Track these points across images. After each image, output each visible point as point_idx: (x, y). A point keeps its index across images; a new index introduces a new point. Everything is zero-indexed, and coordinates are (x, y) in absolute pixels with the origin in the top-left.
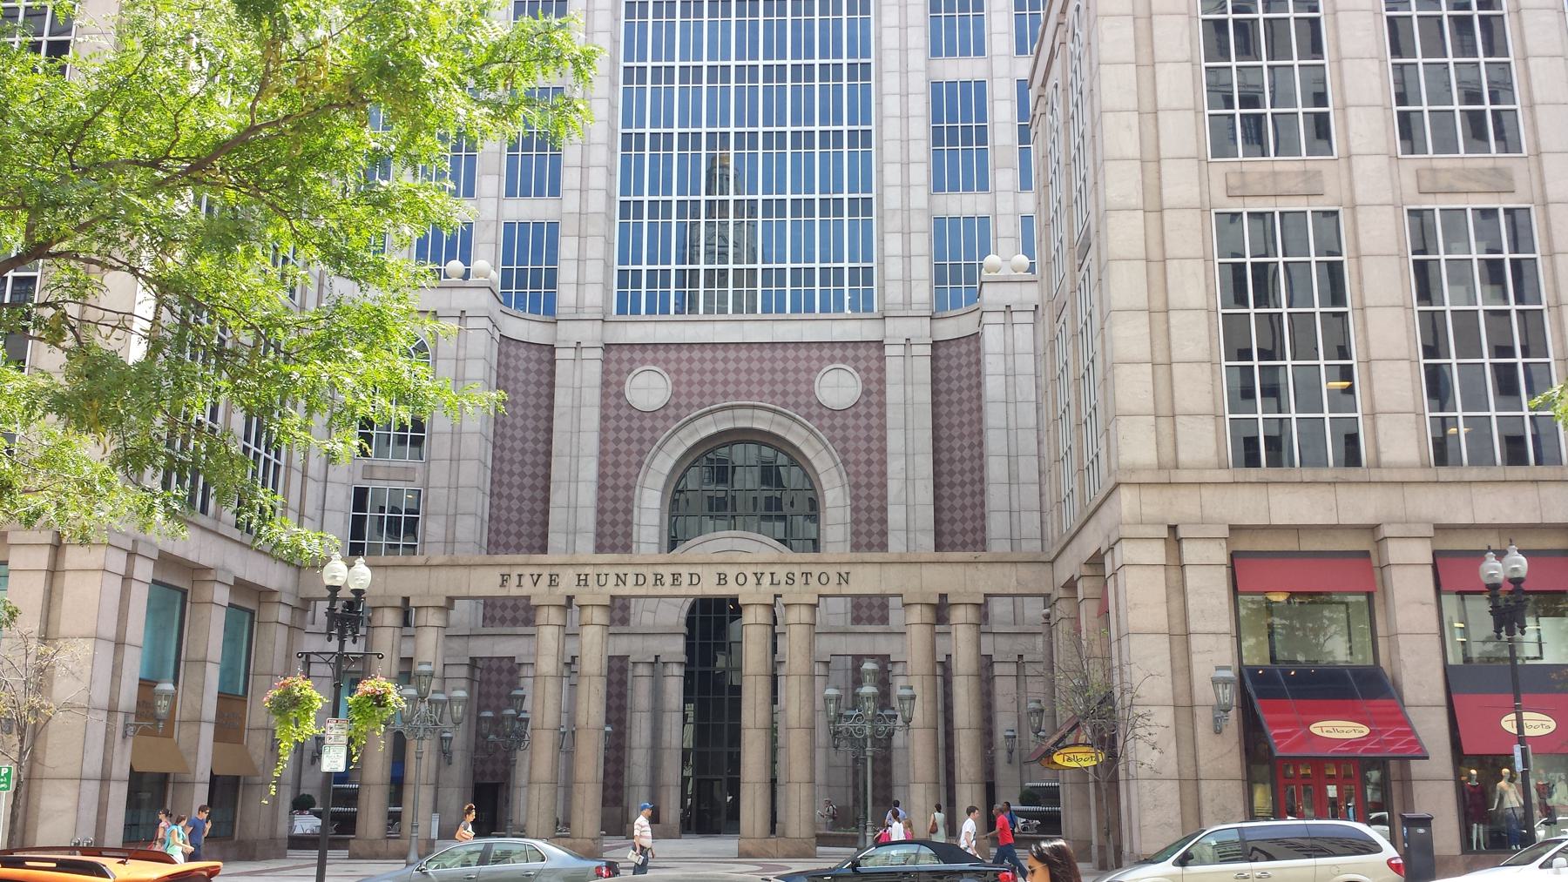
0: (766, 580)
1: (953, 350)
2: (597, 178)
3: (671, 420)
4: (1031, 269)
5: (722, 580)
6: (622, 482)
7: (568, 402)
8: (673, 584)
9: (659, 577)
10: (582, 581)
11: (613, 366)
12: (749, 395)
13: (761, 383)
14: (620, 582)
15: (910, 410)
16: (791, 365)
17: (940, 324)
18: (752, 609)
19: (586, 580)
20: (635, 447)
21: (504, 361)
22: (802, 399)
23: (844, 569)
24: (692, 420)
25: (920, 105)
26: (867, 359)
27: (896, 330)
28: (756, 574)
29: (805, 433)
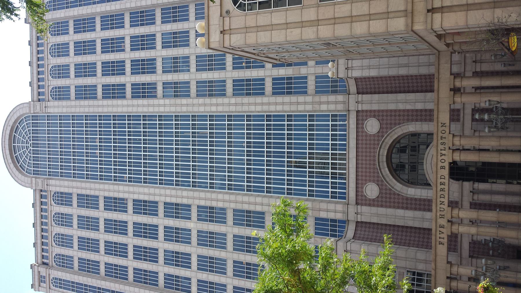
0: (443, 152)
1: (360, 87)
4: (333, 61)
5: (443, 168)
6: (405, 201)
7: (376, 218)
8: (444, 185)
9: (441, 190)
10: (442, 217)
11: (364, 202)
12: (374, 156)
13: (370, 152)
15: (381, 102)
16: (364, 142)
17: (351, 91)
19: (442, 215)
20: (392, 196)
21: (361, 239)
22: (376, 138)
23: (440, 125)
24: (383, 176)
25: (279, 99)
26: (362, 116)
27: (353, 107)
28: (441, 156)
29: (388, 137)
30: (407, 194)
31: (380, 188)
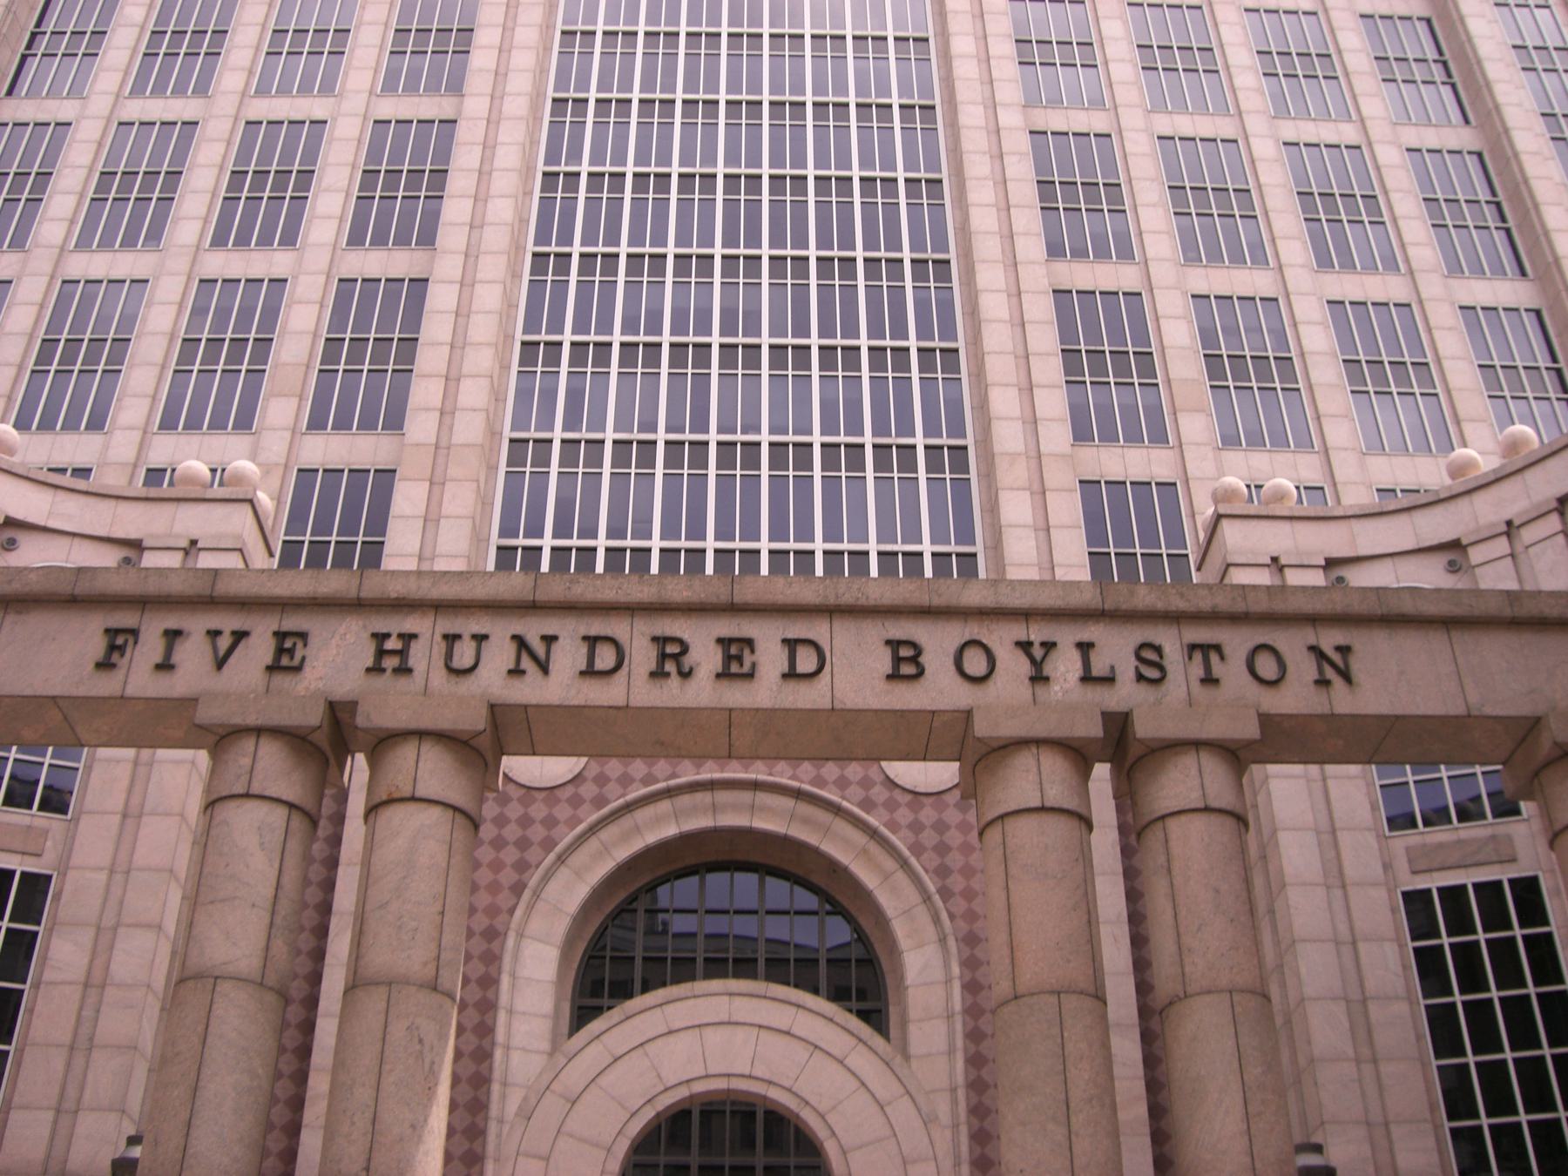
2: (473, 393)
3: (586, 806)
9: (672, 649)
14: (527, 663)
18: (1024, 761)
19: (402, 653)
24: (629, 807)
29: (859, 838)
30: (521, 935)
31: (558, 792)
